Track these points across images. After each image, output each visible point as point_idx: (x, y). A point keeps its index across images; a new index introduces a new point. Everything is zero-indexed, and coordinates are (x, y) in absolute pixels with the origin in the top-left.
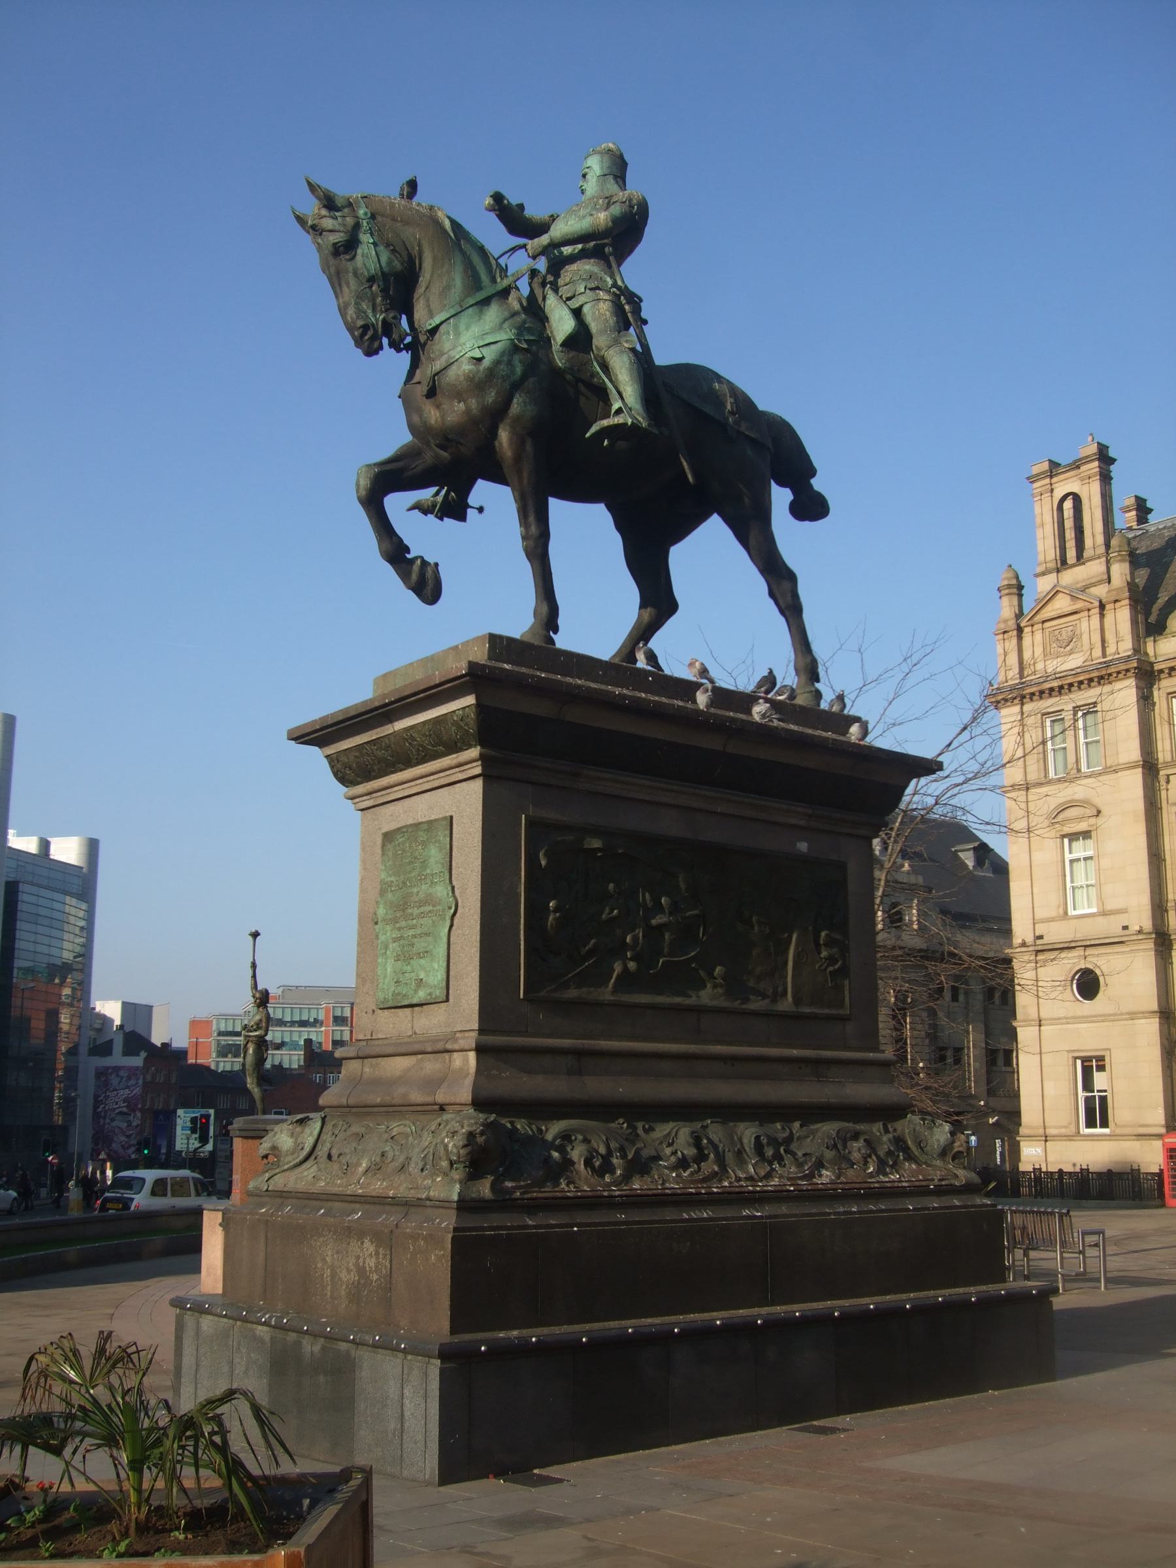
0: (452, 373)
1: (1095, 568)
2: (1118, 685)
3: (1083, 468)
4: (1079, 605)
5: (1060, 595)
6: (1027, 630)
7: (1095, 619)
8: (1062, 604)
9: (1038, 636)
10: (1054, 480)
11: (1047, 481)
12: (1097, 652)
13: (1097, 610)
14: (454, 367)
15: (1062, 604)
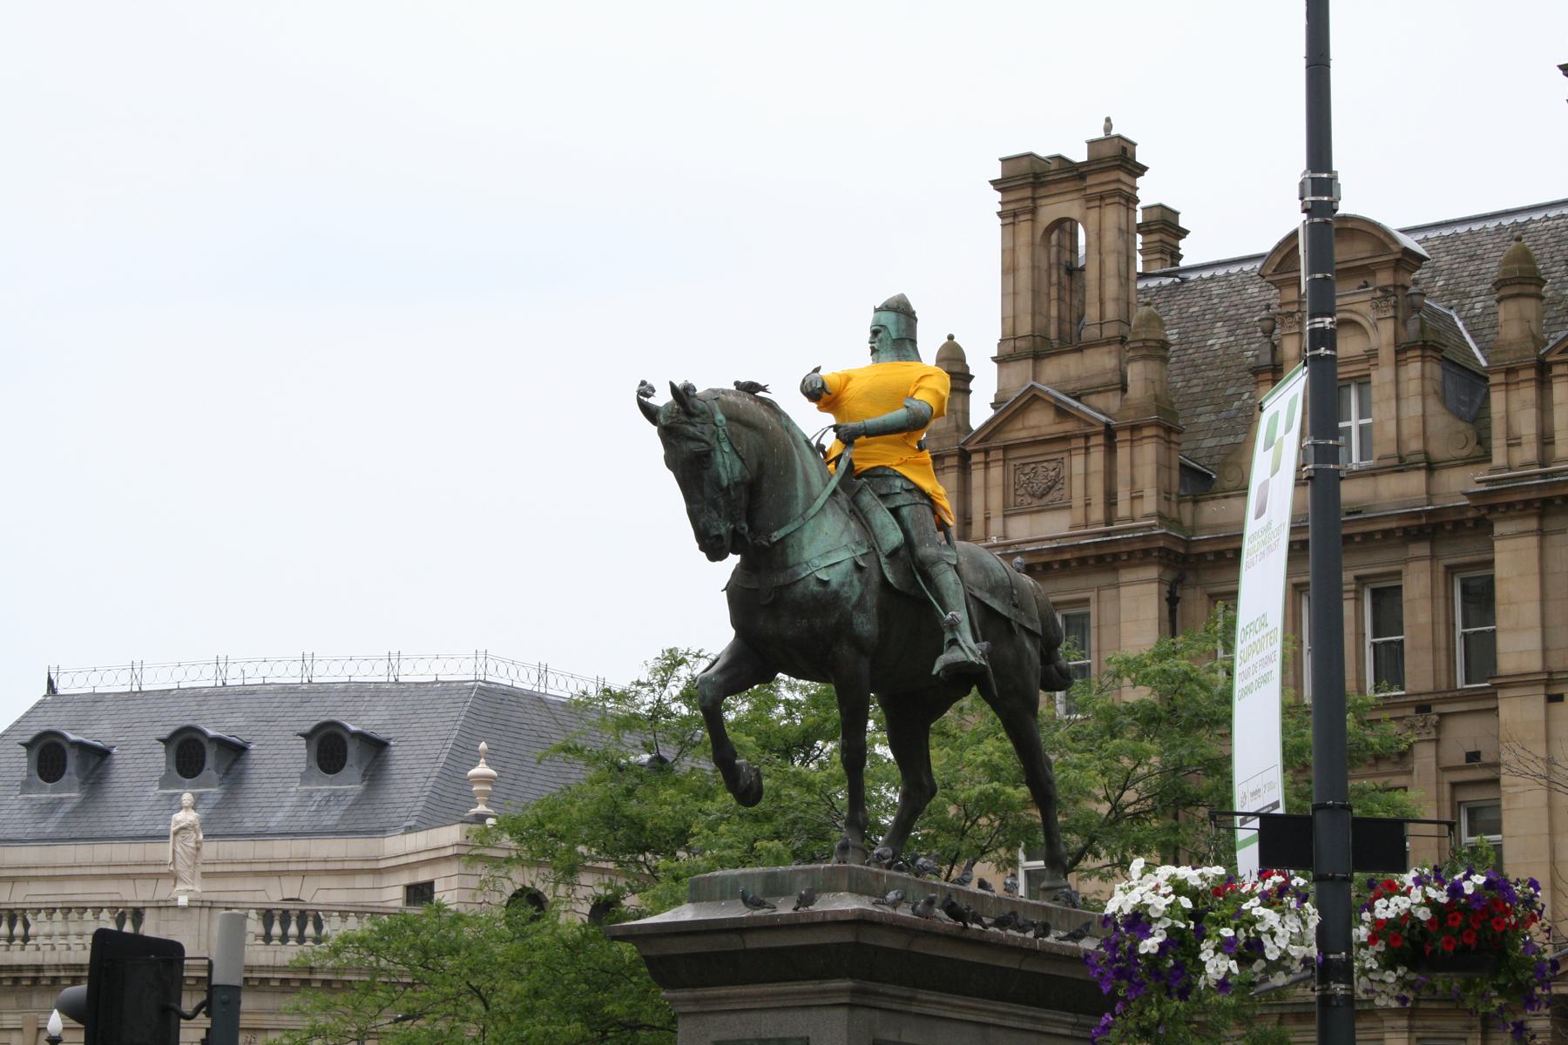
0: (800, 588)
1: (1101, 362)
2: (1126, 576)
3: (1090, 180)
4: (1069, 426)
5: (1037, 406)
6: (976, 458)
7: (1097, 457)
8: (1040, 422)
9: (996, 472)
10: (1042, 192)
11: (1027, 193)
12: (1097, 513)
13: (1100, 440)
14: (801, 585)
15: (1040, 422)
